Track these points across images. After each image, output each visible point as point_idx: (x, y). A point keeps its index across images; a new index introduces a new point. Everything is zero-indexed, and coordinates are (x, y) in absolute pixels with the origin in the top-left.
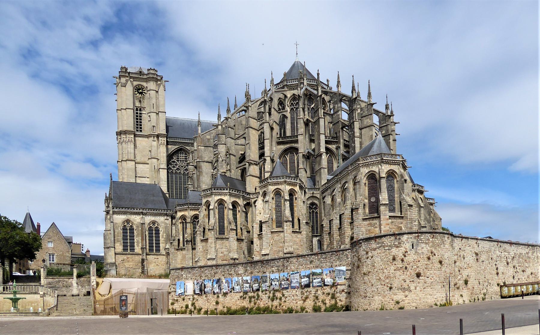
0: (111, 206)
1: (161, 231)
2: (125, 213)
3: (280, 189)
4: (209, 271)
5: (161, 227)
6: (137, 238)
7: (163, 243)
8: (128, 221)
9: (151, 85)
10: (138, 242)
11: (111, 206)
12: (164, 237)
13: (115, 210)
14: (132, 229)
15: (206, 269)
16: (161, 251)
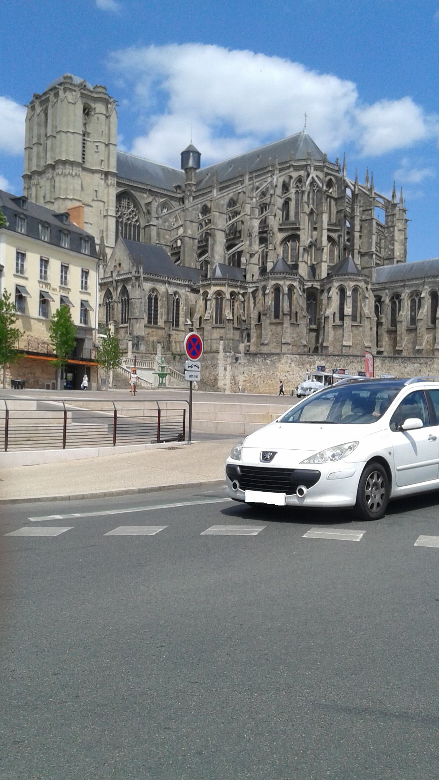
0: (141, 270)
1: (182, 304)
2: (152, 280)
3: (359, 286)
4: (345, 360)
5: (181, 298)
6: (161, 310)
7: (183, 317)
8: (154, 290)
9: (99, 107)
10: (162, 314)
11: (141, 270)
12: (184, 310)
13: (146, 276)
14: (156, 299)
15: (342, 358)
16: (180, 326)
